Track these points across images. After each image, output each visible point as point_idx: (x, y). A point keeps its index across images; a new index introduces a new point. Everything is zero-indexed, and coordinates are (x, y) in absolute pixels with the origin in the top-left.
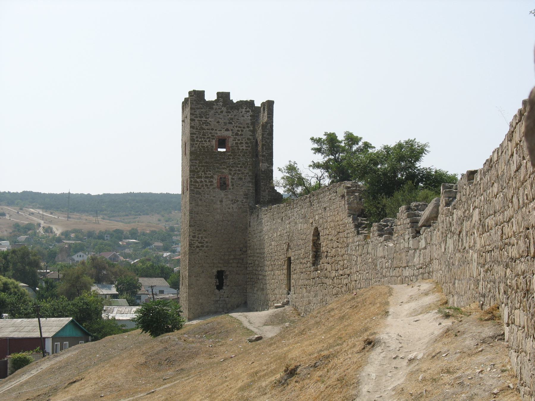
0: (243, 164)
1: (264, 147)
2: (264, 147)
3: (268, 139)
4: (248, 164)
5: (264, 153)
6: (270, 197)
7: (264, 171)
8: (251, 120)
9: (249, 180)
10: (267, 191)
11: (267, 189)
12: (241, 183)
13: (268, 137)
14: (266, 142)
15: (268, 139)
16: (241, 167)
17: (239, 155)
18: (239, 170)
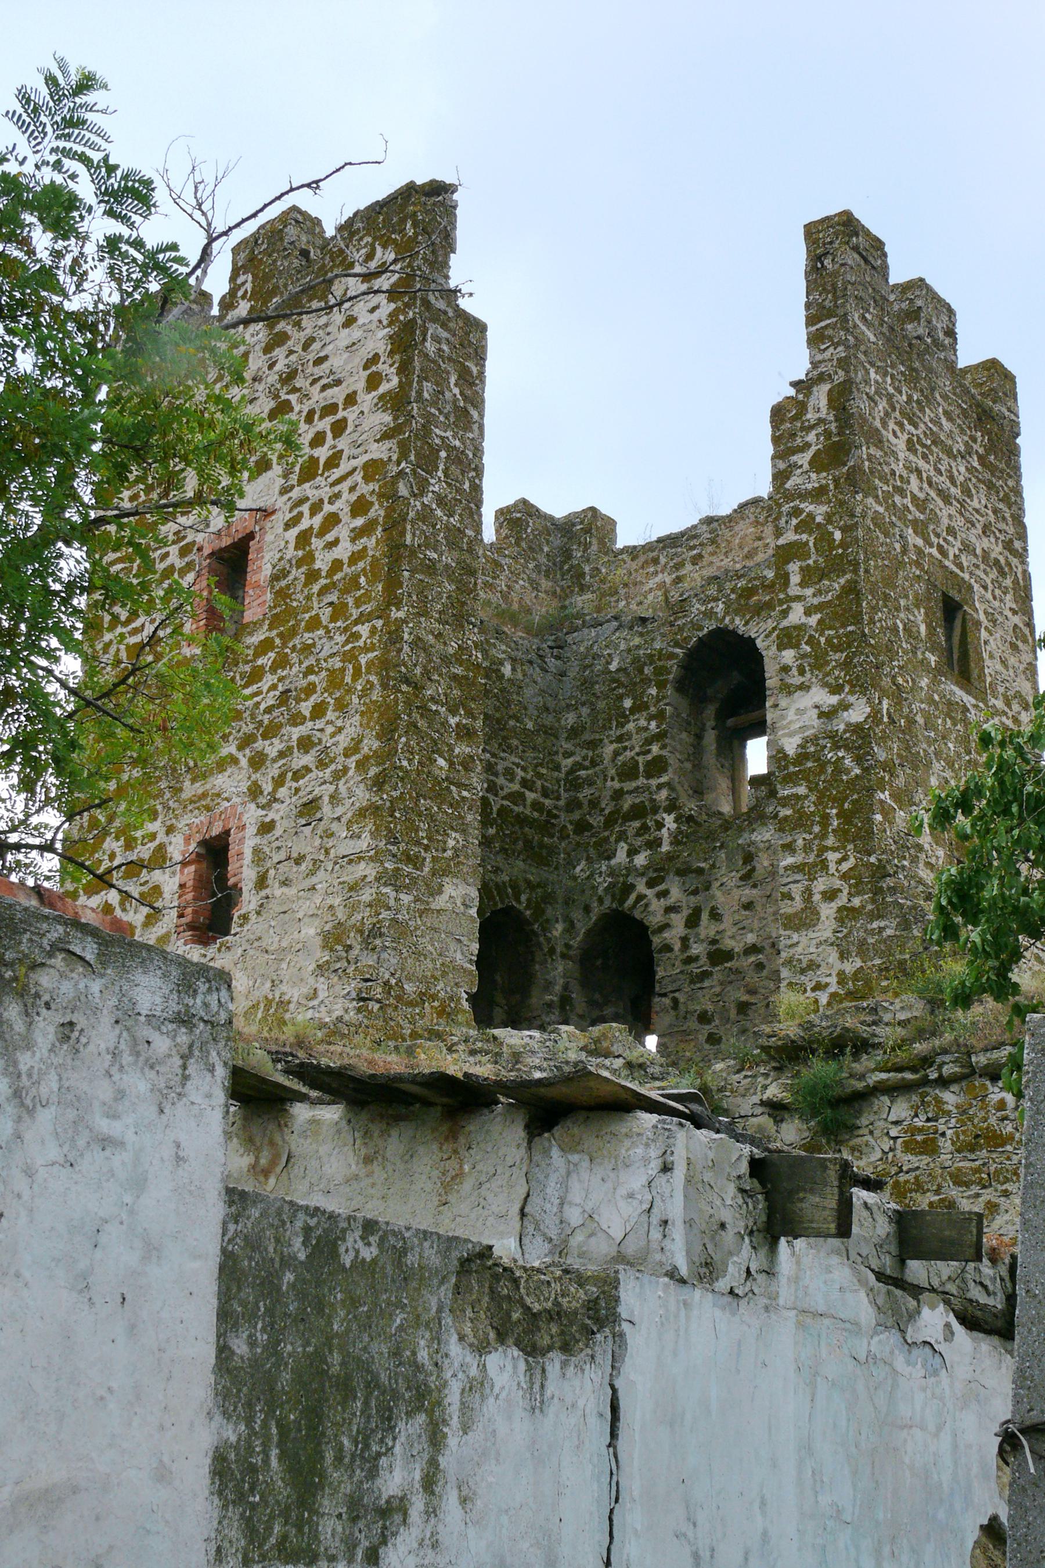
0: (335, 679)
1: (794, 567)
2: (794, 567)
3: (818, 494)
4: (357, 674)
5: (796, 615)
6: (850, 967)
7: (802, 757)
8: (393, 316)
9: (363, 796)
10: (828, 911)
11: (830, 895)
12: (307, 843)
13: (815, 480)
14: (807, 525)
15: (818, 494)
16: (318, 711)
17: (314, 624)
18: (305, 744)
